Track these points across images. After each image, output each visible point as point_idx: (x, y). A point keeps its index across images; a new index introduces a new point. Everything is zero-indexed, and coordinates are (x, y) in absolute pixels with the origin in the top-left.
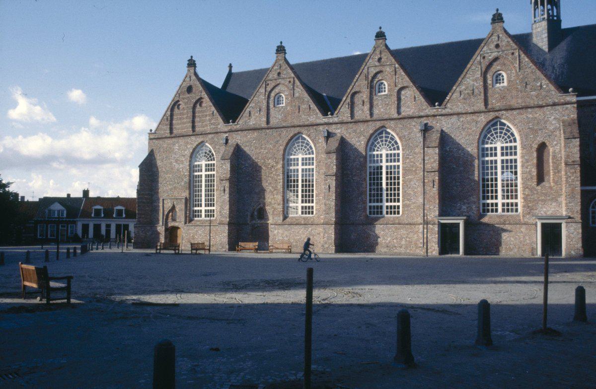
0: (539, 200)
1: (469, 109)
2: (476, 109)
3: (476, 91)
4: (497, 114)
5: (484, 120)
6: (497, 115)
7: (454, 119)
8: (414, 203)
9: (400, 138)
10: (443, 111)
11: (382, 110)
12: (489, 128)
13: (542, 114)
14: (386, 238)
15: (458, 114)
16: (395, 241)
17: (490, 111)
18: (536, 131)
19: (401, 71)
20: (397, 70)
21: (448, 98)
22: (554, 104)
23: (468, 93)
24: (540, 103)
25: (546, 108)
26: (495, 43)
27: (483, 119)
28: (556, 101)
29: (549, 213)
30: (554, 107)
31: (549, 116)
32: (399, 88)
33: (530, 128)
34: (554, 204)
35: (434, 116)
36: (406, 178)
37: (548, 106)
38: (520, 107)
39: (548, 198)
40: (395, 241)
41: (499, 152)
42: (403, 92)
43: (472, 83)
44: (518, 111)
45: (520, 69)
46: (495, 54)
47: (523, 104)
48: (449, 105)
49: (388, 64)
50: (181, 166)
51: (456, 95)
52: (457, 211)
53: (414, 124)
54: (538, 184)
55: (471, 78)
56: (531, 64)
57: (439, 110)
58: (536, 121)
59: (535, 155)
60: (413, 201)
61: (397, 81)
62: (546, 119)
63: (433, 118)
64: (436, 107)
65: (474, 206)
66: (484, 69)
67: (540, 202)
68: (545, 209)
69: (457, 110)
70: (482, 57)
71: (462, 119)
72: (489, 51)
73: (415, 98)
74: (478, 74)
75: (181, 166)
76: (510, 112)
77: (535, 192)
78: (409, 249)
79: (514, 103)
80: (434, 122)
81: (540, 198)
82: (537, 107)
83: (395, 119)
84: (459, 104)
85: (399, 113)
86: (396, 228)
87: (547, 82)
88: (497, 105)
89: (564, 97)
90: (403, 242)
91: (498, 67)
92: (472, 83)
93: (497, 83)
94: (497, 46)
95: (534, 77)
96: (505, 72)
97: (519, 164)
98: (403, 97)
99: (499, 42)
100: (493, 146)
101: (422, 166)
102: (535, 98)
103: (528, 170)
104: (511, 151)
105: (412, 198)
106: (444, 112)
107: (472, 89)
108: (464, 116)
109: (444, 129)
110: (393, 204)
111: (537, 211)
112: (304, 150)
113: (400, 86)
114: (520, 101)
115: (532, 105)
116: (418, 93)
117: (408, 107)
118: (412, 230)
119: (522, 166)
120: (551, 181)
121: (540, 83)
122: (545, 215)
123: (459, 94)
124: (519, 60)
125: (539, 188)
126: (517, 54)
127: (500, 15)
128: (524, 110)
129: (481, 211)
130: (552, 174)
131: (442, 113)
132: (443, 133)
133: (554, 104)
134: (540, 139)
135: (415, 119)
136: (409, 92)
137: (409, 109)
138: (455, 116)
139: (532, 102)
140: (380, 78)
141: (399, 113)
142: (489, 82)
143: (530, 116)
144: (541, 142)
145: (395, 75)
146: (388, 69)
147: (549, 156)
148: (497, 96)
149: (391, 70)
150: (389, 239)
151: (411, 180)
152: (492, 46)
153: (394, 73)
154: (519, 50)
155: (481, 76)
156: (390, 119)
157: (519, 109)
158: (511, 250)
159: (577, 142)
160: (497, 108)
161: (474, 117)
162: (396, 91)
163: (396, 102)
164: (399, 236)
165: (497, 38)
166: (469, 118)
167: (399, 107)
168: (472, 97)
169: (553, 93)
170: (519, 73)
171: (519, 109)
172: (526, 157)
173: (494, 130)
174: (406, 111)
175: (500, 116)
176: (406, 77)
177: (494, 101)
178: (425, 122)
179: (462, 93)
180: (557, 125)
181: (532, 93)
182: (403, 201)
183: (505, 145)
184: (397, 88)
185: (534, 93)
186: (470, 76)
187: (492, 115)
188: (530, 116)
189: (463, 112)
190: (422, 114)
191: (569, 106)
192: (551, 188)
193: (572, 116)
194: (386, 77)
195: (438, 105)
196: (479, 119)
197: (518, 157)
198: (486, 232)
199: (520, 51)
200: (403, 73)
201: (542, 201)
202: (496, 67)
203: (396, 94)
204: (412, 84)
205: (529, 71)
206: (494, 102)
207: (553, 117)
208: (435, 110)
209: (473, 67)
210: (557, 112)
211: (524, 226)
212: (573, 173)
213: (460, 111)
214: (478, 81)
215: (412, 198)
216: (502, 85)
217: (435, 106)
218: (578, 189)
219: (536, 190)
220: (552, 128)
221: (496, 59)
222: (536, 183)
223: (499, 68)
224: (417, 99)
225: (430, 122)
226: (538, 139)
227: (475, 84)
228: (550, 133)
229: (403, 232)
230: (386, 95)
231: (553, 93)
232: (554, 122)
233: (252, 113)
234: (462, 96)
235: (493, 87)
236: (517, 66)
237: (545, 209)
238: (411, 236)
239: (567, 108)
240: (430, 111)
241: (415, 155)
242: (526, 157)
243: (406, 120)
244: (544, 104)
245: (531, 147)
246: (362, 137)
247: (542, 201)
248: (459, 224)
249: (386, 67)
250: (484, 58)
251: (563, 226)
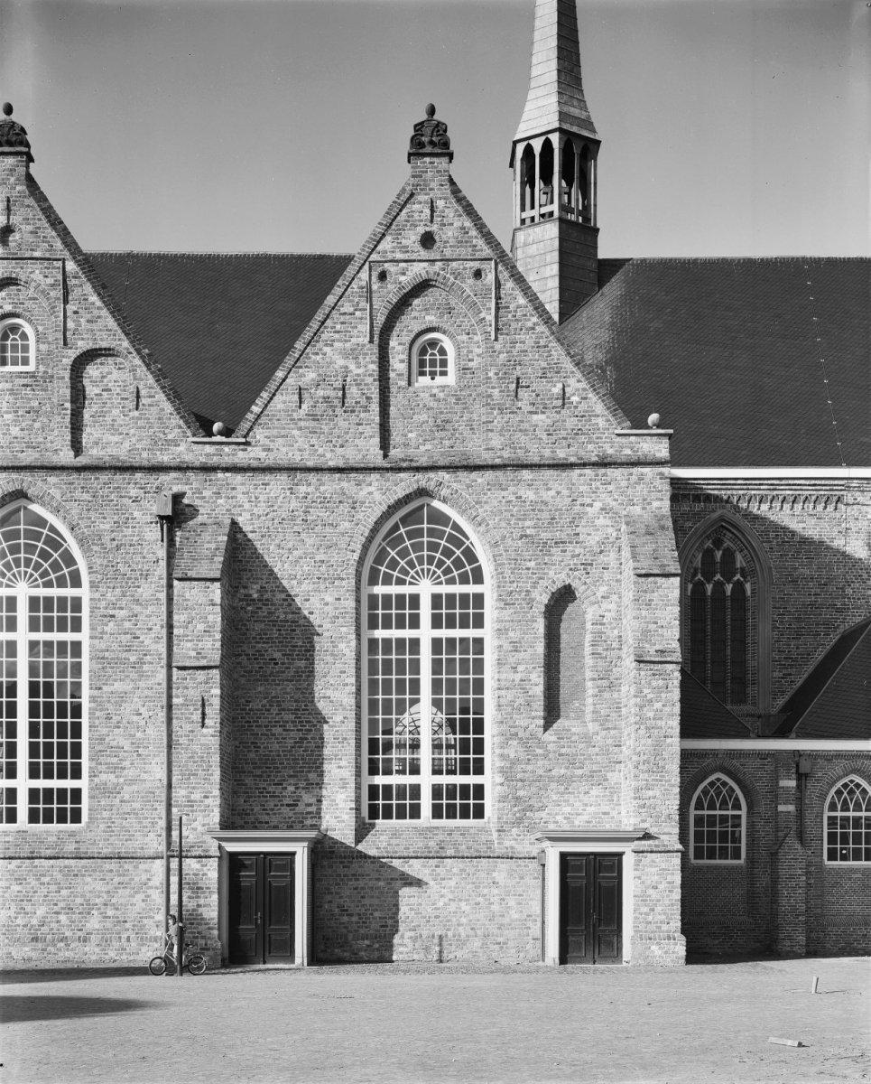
0: (551, 779)
1: (329, 455)
2: (352, 456)
3: (353, 392)
4: (422, 480)
5: (377, 496)
6: (423, 484)
7: (278, 483)
8: (132, 782)
9: (82, 542)
10: (241, 454)
11: (15, 431)
12: (396, 528)
13: (565, 492)
14: (29, 908)
15: (291, 469)
16: (63, 918)
17: (400, 470)
18: (545, 547)
19: (88, 288)
20: (72, 282)
21: (255, 409)
22: (604, 463)
23: (326, 399)
24: (561, 454)
25: (577, 471)
26: (421, 230)
27: (377, 494)
28: (610, 451)
29: (580, 823)
30: (602, 471)
31: (588, 501)
32: (78, 352)
33: (526, 536)
34: (595, 791)
35: (207, 469)
36: (105, 688)
37: (584, 465)
38: (498, 461)
39: (580, 772)
40: (63, 918)
41: (425, 612)
42: (92, 371)
43: (341, 362)
44: (489, 475)
45: (497, 329)
46: (418, 271)
47: (506, 454)
48: (259, 434)
49: (36, 254)
51: (283, 401)
52: (285, 810)
53: (133, 492)
54: (546, 727)
55: (336, 344)
56: (535, 319)
57: (226, 449)
58: (546, 515)
59: (540, 626)
60: (131, 773)
61: (70, 325)
62: (577, 508)
63: (202, 476)
64: (214, 439)
65: (343, 796)
66: (380, 319)
67: (553, 785)
68: (568, 809)
70: (375, 275)
71: (303, 489)
72: (399, 256)
73: (138, 397)
74: (362, 332)
76: (462, 475)
77: (539, 751)
78: (116, 944)
79: (477, 448)
80: (206, 493)
81: (553, 773)
82: (550, 466)
83: (63, 468)
84: (296, 432)
85: (77, 447)
86: (67, 872)
87: (584, 385)
88: (422, 448)
89: (632, 438)
90: (94, 923)
91: (428, 318)
92: (341, 362)
93: (422, 373)
94: (427, 240)
95: (544, 364)
96: (452, 337)
97: (489, 657)
98: (91, 390)
99: (434, 228)
100: (406, 590)
101: (163, 649)
102: (545, 437)
103: (518, 677)
104: (465, 611)
105: (126, 764)
106: (242, 457)
107: (338, 384)
108: (312, 477)
109: (240, 520)
111: (543, 814)
113: (83, 345)
114: (496, 441)
115: (536, 460)
116: (151, 380)
117: (113, 429)
118: (126, 879)
119: (500, 663)
120: (588, 717)
121: (560, 386)
122: (567, 828)
123: (297, 397)
124: (498, 298)
125: (550, 736)
126: (490, 278)
127: (440, 129)
128: (510, 474)
129: (365, 812)
130: (590, 692)
131: (236, 461)
132: (239, 536)
133: (604, 463)
134: (557, 578)
135: (138, 475)
136: (115, 375)
137: (116, 438)
138: (283, 477)
139: (534, 448)
141: (77, 447)
142: (398, 364)
143: (530, 495)
144: (559, 585)
145: (66, 301)
146: (37, 276)
147: (582, 635)
148: (424, 417)
149: (50, 281)
150: (41, 911)
151: (122, 697)
152: (412, 238)
153: (58, 293)
154: (496, 264)
155: (371, 341)
156: (42, 468)
157: (494, 467)
158: (462, 943)
159: (672, 589)
160: (424, 461)
161: (344, 484)
162: (68, 362)
163: (68, 405)
164: (79, 900)
165: (428, 211)
166: (331, 484)
167: (76, 427)
168: (339, 411)
169: (601, 422)
170: (498, 346)
171: (494, 467)
172: (511, 634)
173: (411, 535)
174: (102, 442)
175: (431, 486)
176: (105, 312)
177: (410, 435)
178: (176, 489)
179: (306, 395)
180: (610, 530)
181: (535, 417)
182: (92, 775)
184: (73, 354)
185: (542, 417)
186: (337, 336)
187: (404, 484)
188: (530, 495)
189: (310, 464)
190: (165, 458)
191: (646, 470)
192: (587, 739)
193: (656, 504)
194: (29, 304)
195: (221, 433)
196: (363, 493)
197: (487, 633)
198: (381, 884)
199: (500, 268)
200: (94, 298)
201: (561, 780)
202: (419, 316)
203: (67, 375)
204: (126, 344)
205: (529, 340)
206: (411, 440)
207: (598, 505)
208: (208, 449)
209: (347, 308)
210: (610, 488)
211: (503, 865)
212: (658, 690)
213: (296, 458)
214: (361, 360)
215: (126, 764)
216: (439, 380)
217: (210, 434)
218: (674, 745)
219: (540, 744)
220: (593, 541)
221: (422, 287)
222: (542, 722)
223: (431, 319)
224: (143, 401)
225: (193, 489)
226: (551, 573)
227: (352, 367)
228: (589, 558)
229: (92, 884)
230: (32, 375)
231: (601, 422)
232: (601, 521)
234: (304, 406)
235: (409, 384)
236: (491, 318)
237: (568, 809)
238: (122, 901)
240: (189, 449)
241: (137, 609)
242: (511, 634)
243: (104, 477)
244: (573, 459)
245: (530, 602)
247: (561, 780)
248: (293, 854)
249: (29, 265)
250: (383, 276)
251: (628, 862)
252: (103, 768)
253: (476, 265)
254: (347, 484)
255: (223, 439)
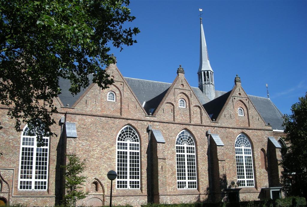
48: (220, 121)
50: (11, 137)
69: (224, 125)
75: (11, 137)
106: (217, 125)
110: (182, 181)
112: (126, 137)
113: (194, 105)
140: (182, 97)
183: (132, 143)
213: (226, 126)
233: (89, 102)
239: (270, 132)
246: (173, 134)
252: (201, 178)
253: (246, 99)
254: (233, 130)
255: (215, 122)
